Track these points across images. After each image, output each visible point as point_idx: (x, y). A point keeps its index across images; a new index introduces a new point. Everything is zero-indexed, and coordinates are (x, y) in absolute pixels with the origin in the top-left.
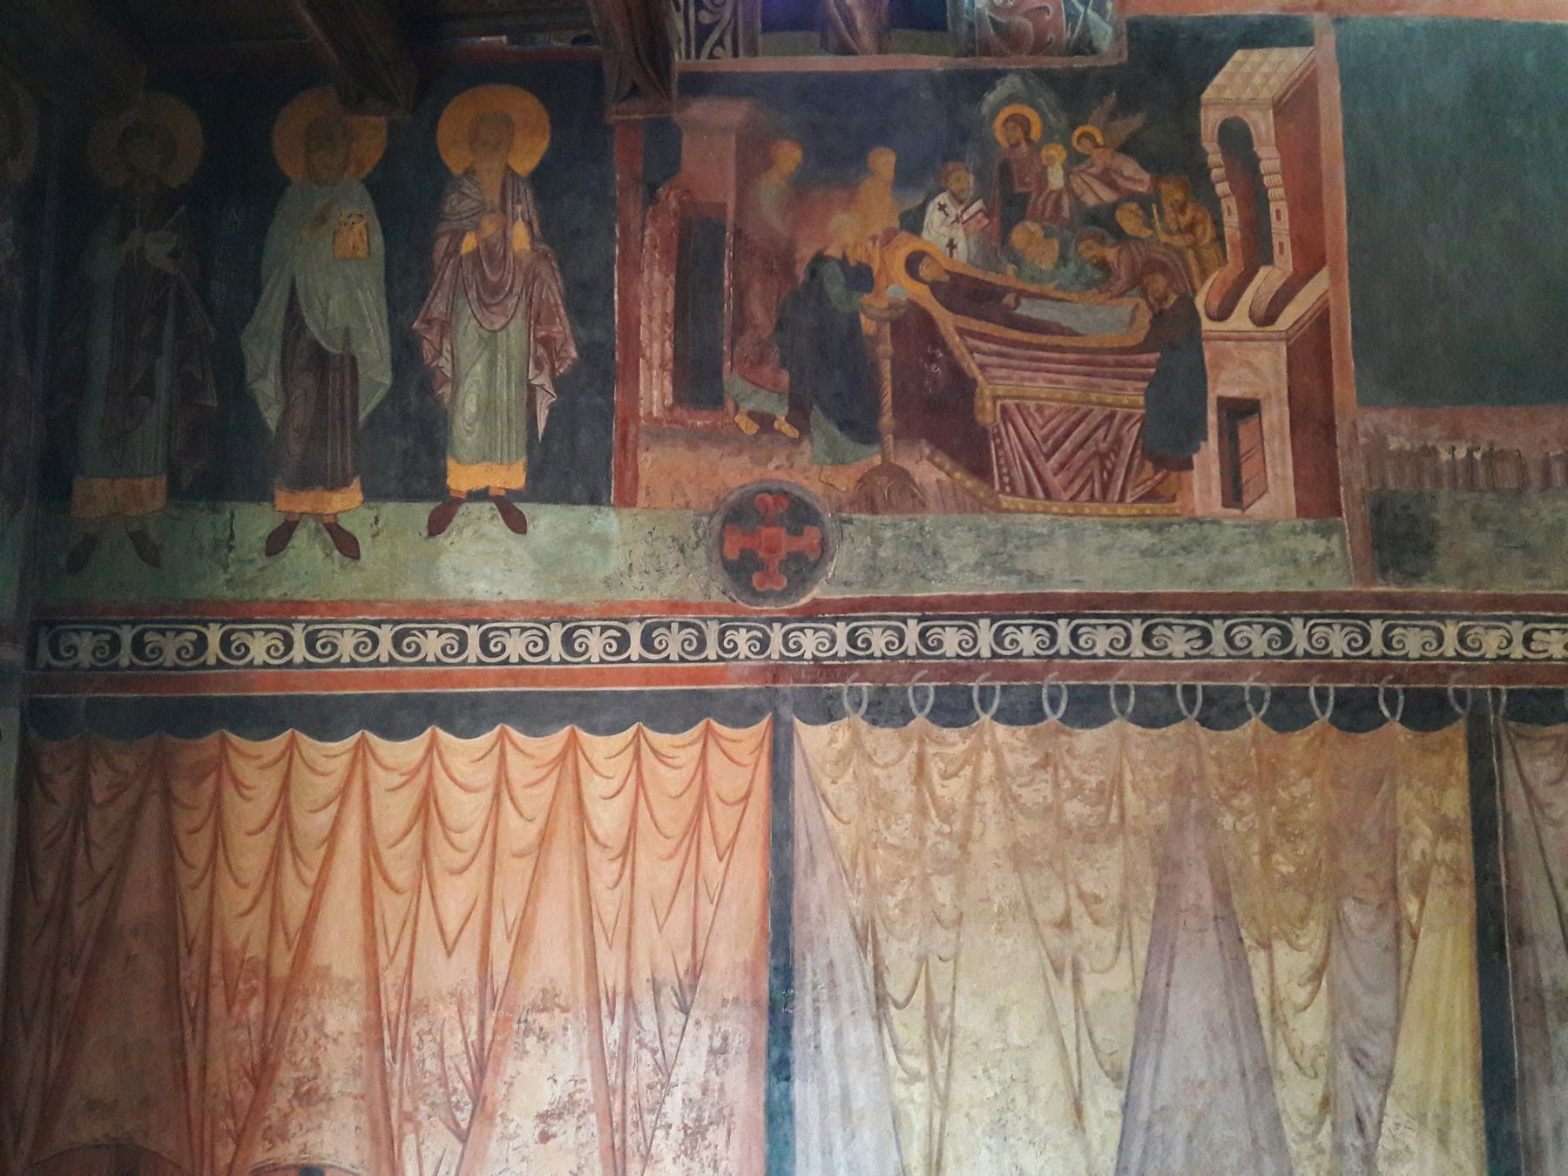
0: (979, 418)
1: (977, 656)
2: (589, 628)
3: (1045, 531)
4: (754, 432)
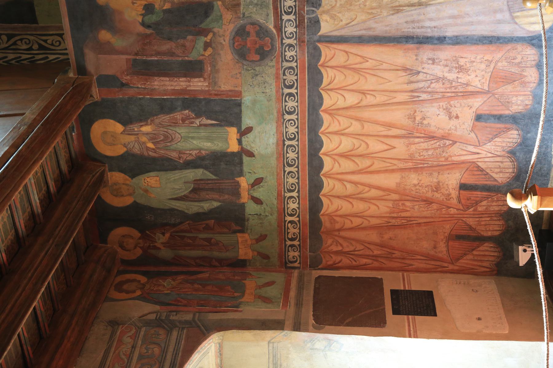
2: (285, 106)
4: (211, 49)
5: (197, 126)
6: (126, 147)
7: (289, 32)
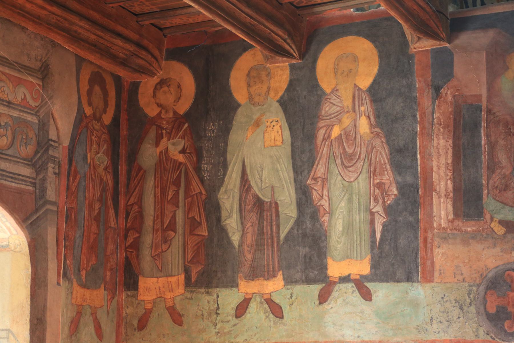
5: (371, 208)
6: (332, 92)
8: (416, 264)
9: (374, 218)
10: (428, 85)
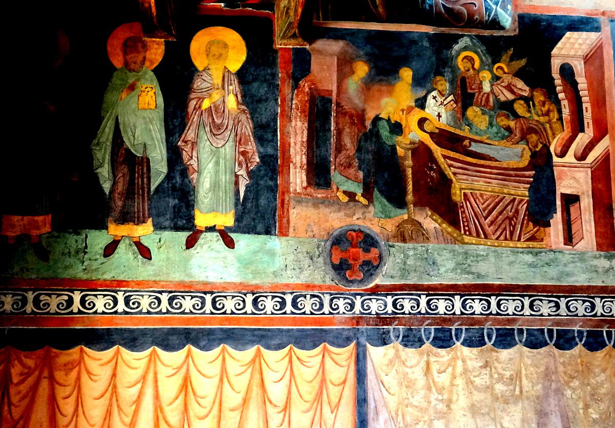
0: (454, 198)
1: (454, 314)
2: (266, 297)
3: (485, 253)
6: (204, 70)
7: (371, 304)
8: (274, 220)
9: (239, 180)
10: (288, 76)
